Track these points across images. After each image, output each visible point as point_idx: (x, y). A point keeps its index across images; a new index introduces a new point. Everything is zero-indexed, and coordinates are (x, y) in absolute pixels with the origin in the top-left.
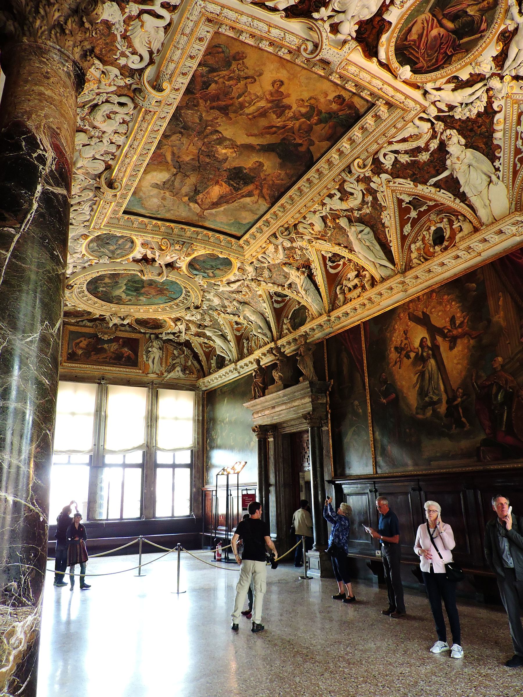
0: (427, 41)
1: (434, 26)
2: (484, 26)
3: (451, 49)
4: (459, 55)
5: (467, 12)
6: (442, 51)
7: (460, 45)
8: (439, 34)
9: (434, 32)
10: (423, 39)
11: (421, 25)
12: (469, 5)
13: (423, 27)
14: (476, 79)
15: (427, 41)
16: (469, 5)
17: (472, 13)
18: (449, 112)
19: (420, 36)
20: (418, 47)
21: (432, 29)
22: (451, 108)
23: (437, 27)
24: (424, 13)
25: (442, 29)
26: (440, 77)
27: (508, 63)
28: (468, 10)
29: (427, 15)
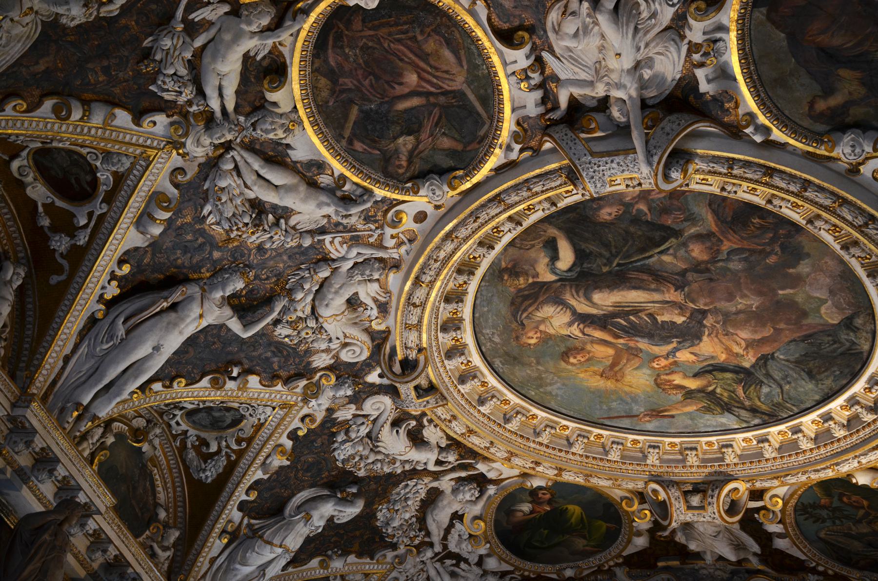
0: (401, 60)
1: (425, 84)
2: (359, 146)
3: (350, 86)
4: (325, 94)
5: (409, 134)
6: (360, 72)
7: (351, 102)
8: (401, 84)
9: (412, 78)
10: (411, 56)
11: (445, 68)
12: (418, 142)
13: (437, 69)
14: (253, 104)
15: (401, 60)
16: (418, 142)
17: (401, 140)
18: (184, 20)
19: (424, 57)
20: (399, 41)
21: (420, 77)
22: (192, 29)
23: (418, 85)
24: (469, 83)
25: (407, 90)
26: (297, 41)
27: (256, 164)
28: (412, 137)
29: (459, 82)
